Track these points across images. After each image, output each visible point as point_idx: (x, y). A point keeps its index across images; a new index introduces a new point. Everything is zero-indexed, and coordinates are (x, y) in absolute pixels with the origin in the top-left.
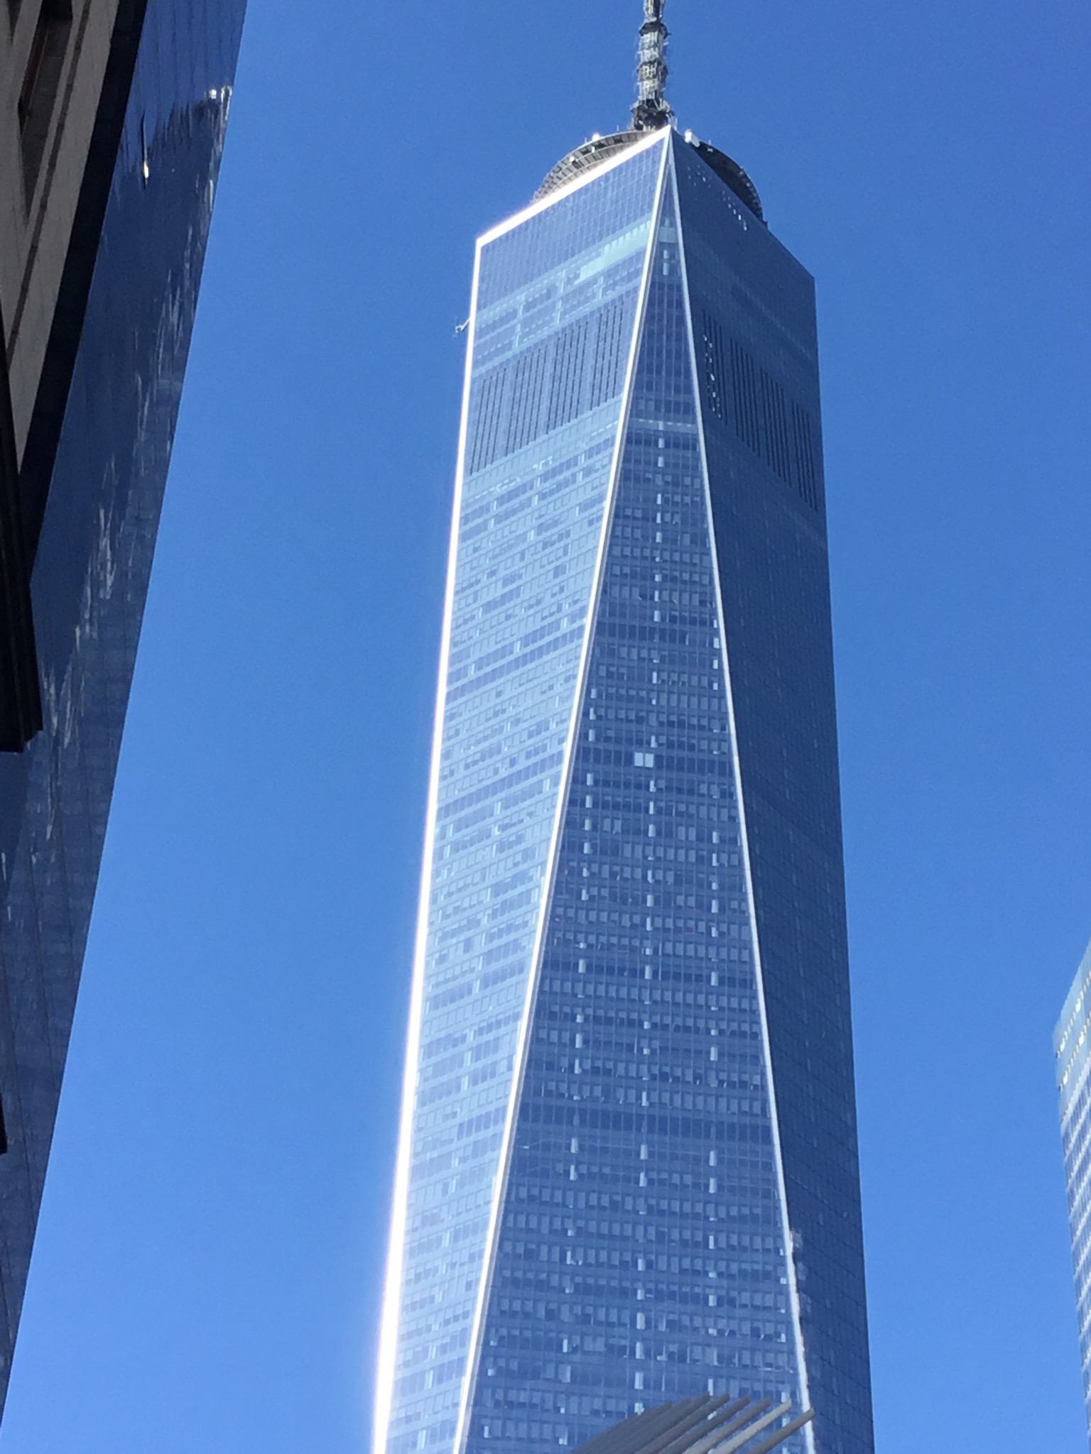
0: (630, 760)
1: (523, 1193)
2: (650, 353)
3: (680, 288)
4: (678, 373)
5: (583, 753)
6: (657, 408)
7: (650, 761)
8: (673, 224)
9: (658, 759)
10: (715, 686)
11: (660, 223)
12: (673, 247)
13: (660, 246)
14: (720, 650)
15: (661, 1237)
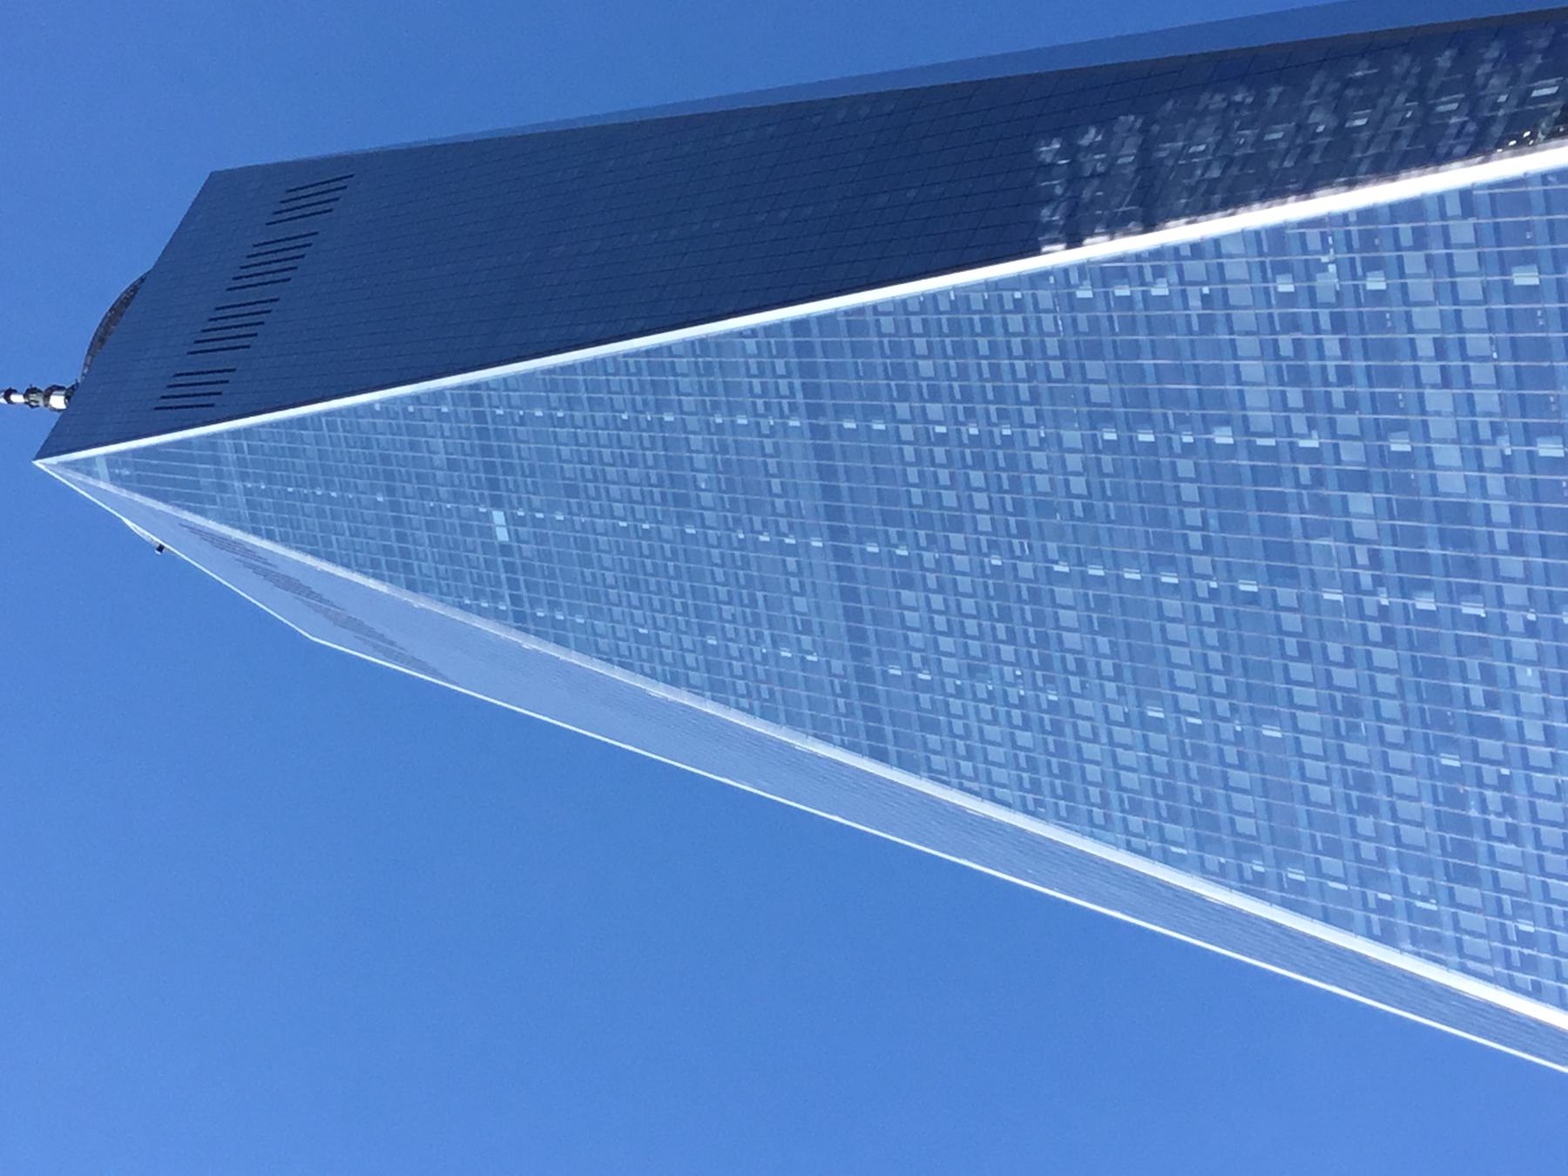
0: (505, 549)
1: (966, 766)
2: (190, 498)
3: (135, 452)
4: (191, 459)
5: (521, 621)
6: (223, 488)
7: (498, 517)
8: (90, 461)
9: (497, 503)
10: (411, 409)
11: (97, 477)
12: (111, 460)
13: (114, 479)
14: (382, 402)
15: (957, 525)
